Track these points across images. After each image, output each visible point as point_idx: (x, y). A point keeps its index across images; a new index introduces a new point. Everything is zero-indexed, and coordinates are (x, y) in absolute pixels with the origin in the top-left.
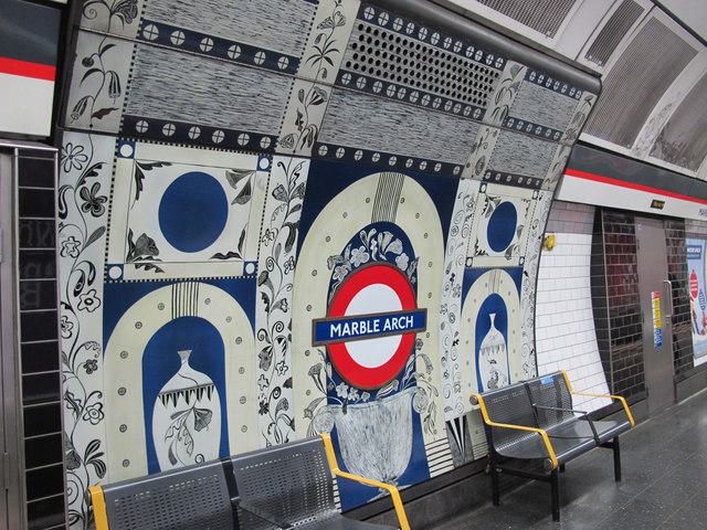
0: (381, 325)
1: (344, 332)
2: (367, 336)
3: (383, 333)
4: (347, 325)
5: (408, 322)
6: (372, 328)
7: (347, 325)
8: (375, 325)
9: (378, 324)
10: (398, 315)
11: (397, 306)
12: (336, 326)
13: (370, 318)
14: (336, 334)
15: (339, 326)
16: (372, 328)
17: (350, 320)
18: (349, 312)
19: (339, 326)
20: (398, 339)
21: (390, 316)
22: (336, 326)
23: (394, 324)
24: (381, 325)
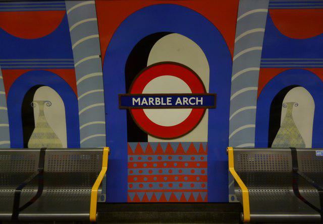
0: (173, 101)
1: (143, 103)
2: (160, 107)
3: (174, 106)
4: (144, 99)
5: (197, 101)
6: (165, 101)
7: (144, 99)
8: (168, 101)
9: (172, 101)
10: (188, 96)
11: (187, 90)
13: (165, 96)
14: (136, 104)
15: (139, 99)
16: (165, 101)
17: (147, 96)
18: (146, 91)
19: (139, 99)
20: (188, 111)
21: (182, 96)
23: (184, 101)
24: (173, 101)
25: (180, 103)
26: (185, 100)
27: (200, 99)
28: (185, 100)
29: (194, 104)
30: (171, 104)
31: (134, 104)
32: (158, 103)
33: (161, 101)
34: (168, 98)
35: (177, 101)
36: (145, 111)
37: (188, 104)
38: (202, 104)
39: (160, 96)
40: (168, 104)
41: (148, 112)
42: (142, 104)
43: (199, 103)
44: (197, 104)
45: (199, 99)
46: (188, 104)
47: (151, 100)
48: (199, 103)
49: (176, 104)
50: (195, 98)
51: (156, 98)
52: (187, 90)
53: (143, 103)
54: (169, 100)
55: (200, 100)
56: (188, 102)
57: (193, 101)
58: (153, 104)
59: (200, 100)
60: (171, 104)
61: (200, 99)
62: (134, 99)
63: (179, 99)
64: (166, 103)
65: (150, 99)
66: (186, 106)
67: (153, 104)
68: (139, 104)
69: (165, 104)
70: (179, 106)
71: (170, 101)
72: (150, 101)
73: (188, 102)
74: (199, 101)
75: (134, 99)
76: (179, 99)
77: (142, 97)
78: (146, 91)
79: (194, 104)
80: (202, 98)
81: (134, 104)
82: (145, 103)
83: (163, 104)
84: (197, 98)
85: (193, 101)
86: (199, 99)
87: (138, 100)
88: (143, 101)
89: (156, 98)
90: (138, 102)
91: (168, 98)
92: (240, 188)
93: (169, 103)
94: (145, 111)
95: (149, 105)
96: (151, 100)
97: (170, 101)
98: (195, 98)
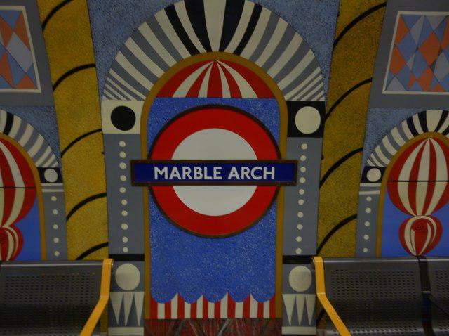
0: (225, 173)
1: (172, 175)
2: (203, 182)
3: (225, 181)
4: (175, 169)
5: (266, 173)
6: (210, 173)
7: (175, 169)
8: (215, 173)
10: (250, 164)
11: (248, 153)
12: (161, 169)
13: (209, 164)
15: (166, 169)
16: (211, 173)
17: (180, 164)
18: (181, 153)
19: (166, 169)
21: (239, 164)
22: (161, 169)
23: (243, 173)
24: (225, 173)
25: (237, 176)
26: (245, 171)
27: (269, 170)
28: (245, 171)
29: (260, 178)
30: (221, 178)
31: (156, 177)
32: (198, 175)
33: (203, 172)
34: (215, 168)
35: (232, 172)
36: (177, 189)
37: (249, 178)
38: (273, 178)
39: (201, 164)
40: (215, 178)
41: (179, 190)
42: (171, 178)
43: (269, 176)
44: (265, 178)
45: (268, 170)
46: (249, 178)
47: (187, 171)
48: (269, 176)
49: (230, 178)
50: (261, 168)
51: (195, 168)
52: (248, 153)
53: (172, 175)
54: (218, 170)
55: (271, 171)
56: (250, 174)
57: (258, 173)
58: (190, 178)
59: (271, 171)
60: (221, 178)
61: (269, 170)
62: (156, 169)
63: (234, 169)
64: (212, 176)
65: (184, 168)
66: (246, 182)
67: (190, 178)
68: (166, 178)
69: (211, 178)
70: (234, 182)
71: (219, 173)
72: (184, 173)
73: (250, 174)
74: (269, 173)
75: (156, 169)
76: (234, 169)
77: (171, 164)
78: (181, 153)
79: (260, 178)
80: (273, 168)
81: (156, 177)
82: (175, 176)
83: (206, 178)
84: (265, 168)
85: (258, 173)
86: (268, 170)
87: (163, 170)
88: (173, 172)
89: (195, 168)
90: (164, 174)
91: (215, 168)
92: (334, 328)
93: (218, 175)
94: (177, 189)
95: (182, 180)
96: (187, 171)
97: (219, 173)
98: (261, 168)
